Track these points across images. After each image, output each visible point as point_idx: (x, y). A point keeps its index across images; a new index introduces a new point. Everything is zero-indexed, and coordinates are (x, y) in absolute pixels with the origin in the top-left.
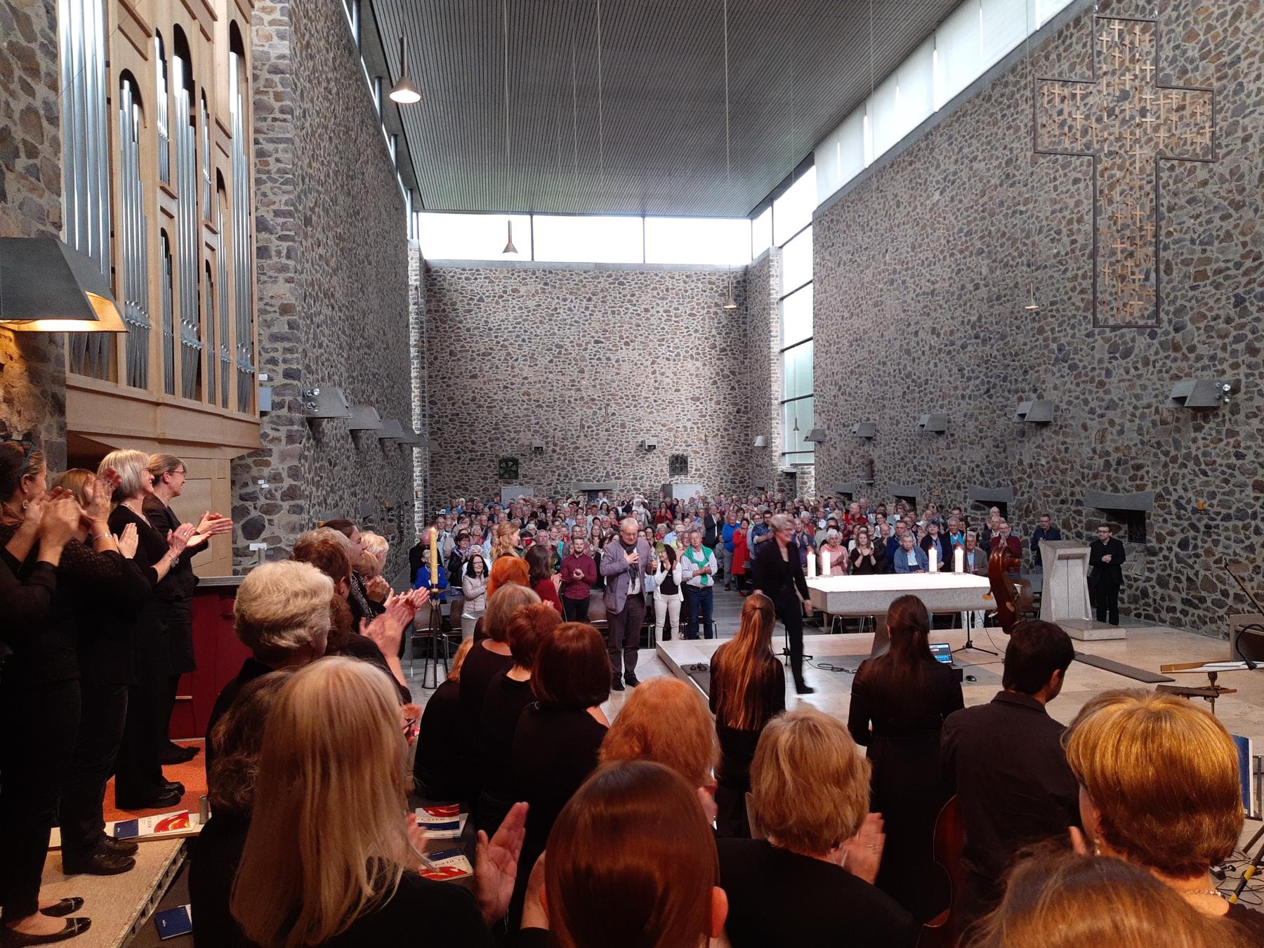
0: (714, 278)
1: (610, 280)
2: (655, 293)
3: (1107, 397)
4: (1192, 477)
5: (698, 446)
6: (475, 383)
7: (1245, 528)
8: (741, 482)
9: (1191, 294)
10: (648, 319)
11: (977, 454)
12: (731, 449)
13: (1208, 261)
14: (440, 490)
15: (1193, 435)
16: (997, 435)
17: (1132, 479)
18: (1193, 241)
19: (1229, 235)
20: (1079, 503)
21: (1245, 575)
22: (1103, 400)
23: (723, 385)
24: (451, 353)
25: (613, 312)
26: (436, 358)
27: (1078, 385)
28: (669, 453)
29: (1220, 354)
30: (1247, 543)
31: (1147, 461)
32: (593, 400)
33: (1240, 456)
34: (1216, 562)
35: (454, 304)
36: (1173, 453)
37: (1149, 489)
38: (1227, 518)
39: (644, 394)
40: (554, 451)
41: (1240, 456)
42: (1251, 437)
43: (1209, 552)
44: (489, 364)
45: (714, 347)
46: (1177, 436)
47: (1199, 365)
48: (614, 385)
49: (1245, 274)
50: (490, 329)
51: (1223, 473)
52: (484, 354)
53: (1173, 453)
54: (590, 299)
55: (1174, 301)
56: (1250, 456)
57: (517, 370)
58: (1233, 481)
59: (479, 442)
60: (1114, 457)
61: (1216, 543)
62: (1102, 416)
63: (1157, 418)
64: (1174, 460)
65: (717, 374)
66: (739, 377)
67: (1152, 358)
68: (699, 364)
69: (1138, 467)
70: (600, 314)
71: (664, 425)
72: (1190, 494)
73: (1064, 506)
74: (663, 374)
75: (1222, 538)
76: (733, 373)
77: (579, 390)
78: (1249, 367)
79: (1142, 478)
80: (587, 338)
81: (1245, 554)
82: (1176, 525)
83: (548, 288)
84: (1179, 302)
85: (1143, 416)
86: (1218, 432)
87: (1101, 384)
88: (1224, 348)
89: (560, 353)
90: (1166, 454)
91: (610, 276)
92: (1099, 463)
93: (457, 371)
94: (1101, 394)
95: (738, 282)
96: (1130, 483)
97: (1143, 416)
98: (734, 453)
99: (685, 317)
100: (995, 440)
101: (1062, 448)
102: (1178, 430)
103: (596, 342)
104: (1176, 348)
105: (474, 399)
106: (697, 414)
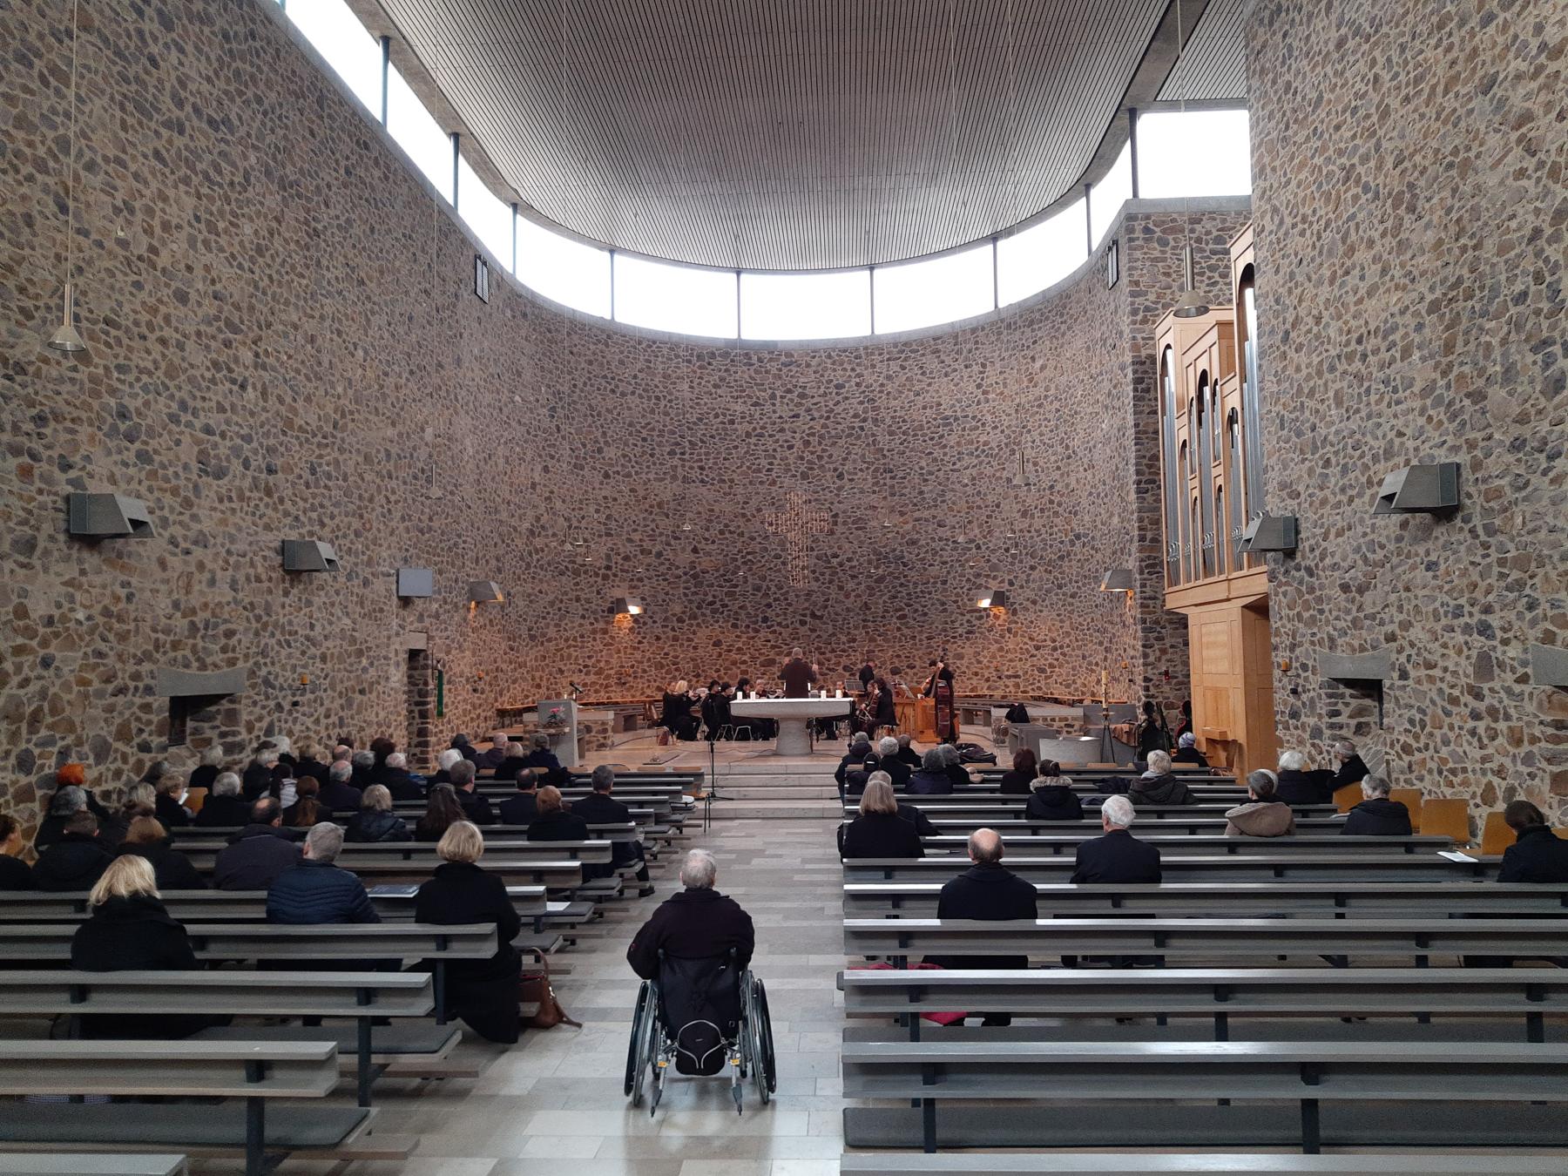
3: (195, 526)
4: (277, 648)
17: (224, 650)
20: (149, 690)
31: (239, 626)
36: (265, 618)
37: (240, 664)
46: (269, 598)
53: (265, 618)
58: (309, 653)
61: (295, 720)
62: (188, 553)
67: (248, 494)
69: (229, 634)
73: (121, 699)
79: (234, 650)
82: (264, 707)
85: (237, 566)
87: (187, 503)
90: (258, 618)
92: (180, 624)
94: (186, 518)
96: (222, 656)
101: (122, 592)
102: (270, 591)
104: (269, 493)
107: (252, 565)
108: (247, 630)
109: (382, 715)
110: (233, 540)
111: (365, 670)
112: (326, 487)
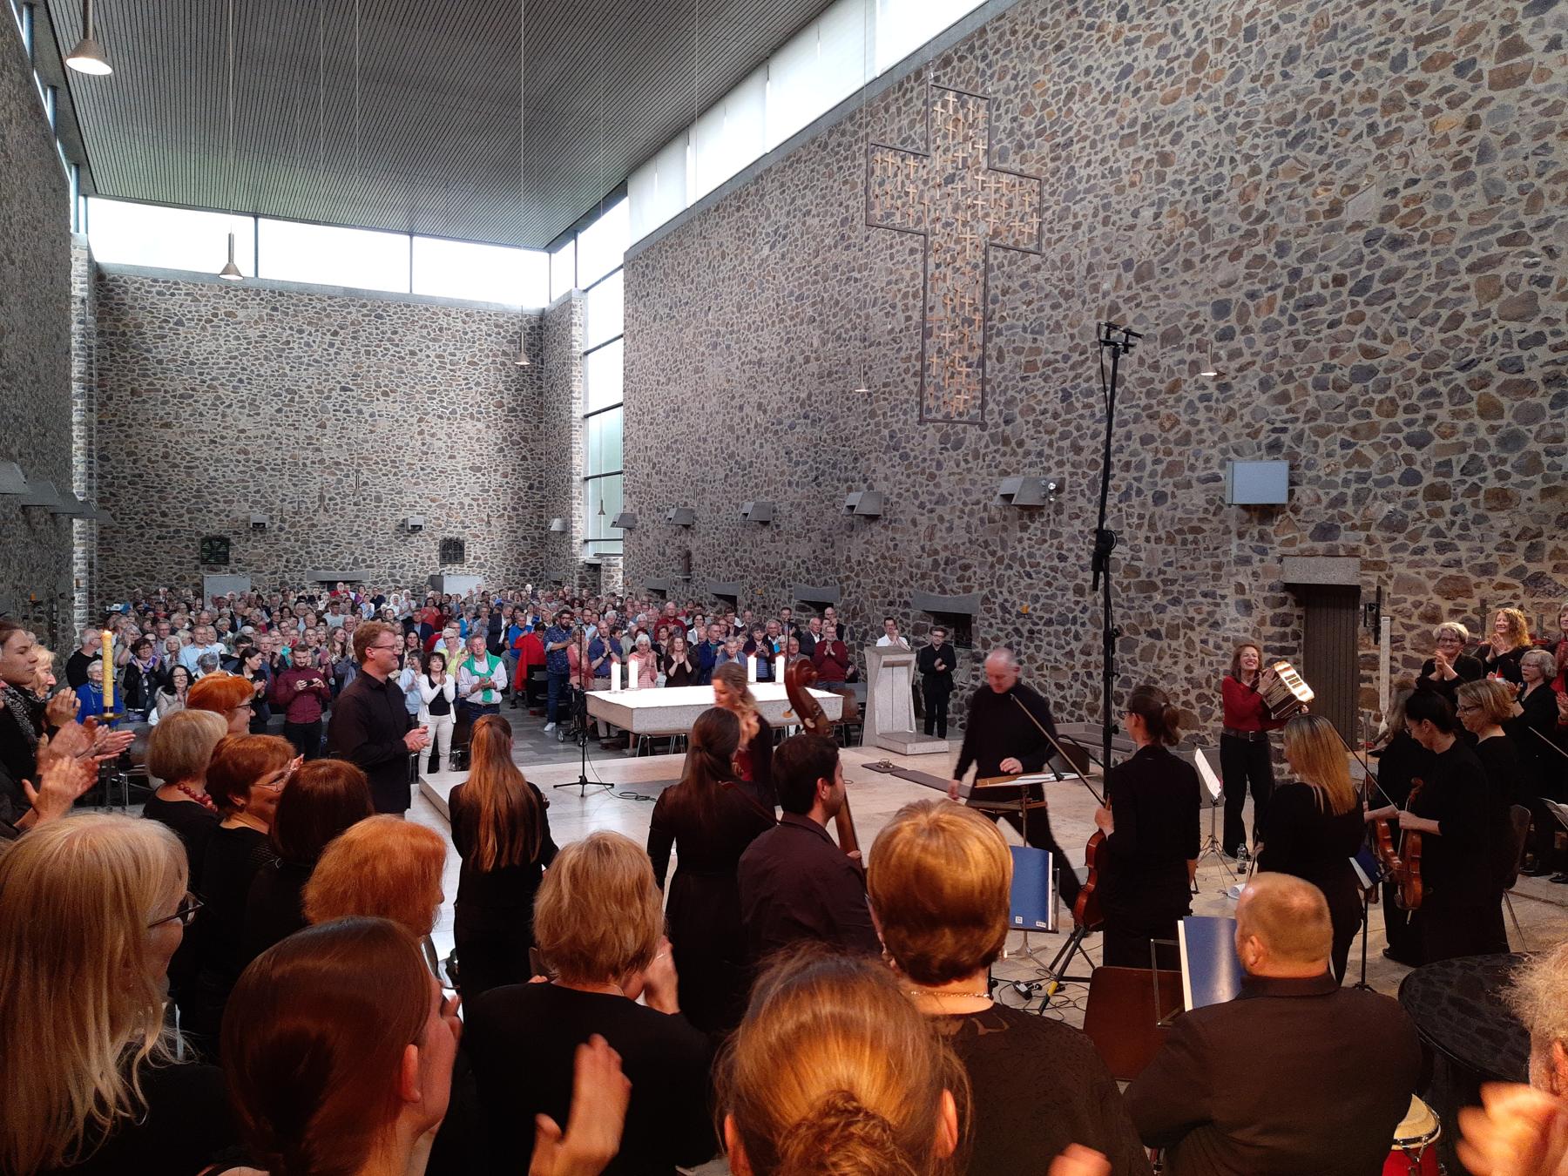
0: (501, 320)
1: (365, 311)
2: (425, 332)
3: (937, 491)
5: (479, 527)
6: (168, 434)
7: (1066, 633)
8: (532, 574)
9: (1021, 385)
10: (414, 364)
11: (803, 549)
12: (520, 533)
13: (1038, 351)
14: (112, 577)
15: (1019, 534)
16: (825, 527)
17: (960, 580)
18: (1025, 329)
19: (1058, 325)
20: (907, 604)
21: (1064, 682)
22: (933, 494)
23: (513, 456)
24: (133, 392)
25: (367, 353)
26: (110, 398)
27: (908, 476)
28: (439, 536)
29: (1047, 451)
30: (1068, 649)
31: (974, 561)
32: (338, 464)
33: (1062, 558)
34: (1037, 669)
35: (140, 326)
36: (1000, 553)
37: (975, 591)
38: (1049, 622)
39: (407, 459)
40: (281, 529)
41: (1062, 558)
42: (1073, 538)
43: (1031, 659)
44: (189, 410)
45: (500, 405)
47: (1027, 461)
48: (366, 446)
49: (1072, 368)
50: (192, 363)
51: (1047, 575)
52: (182, 396)
53: (1000, 553)
54: (335, 333)
55: (1005, 392)
56: (1072, 559)
57: (230, 420)
58: (1055, 584)
59: (172, 513)
60: (943, 555)
62: (932, 511)
63: (985, 515)
64: (1000, 560)
65: (505, 439)
66: (532, 445)
67: (983, 451)
68: (480, 425)
69: (966, 567)
70: (349, 355)
71: (433, 501)
72: (1015, 598)
73: (892, 608)
74: (433, 435)
75: (1044, 644)
76: (525, 439)
77: (318, 450)
78: (1073, 465)
79: (969, 579)
80: (331, 383)
81: (1064, 661)
82: (1001, 630)
83: (278, 315)
84: (1010, 393)
85: (971, 514)
86: (1043, 532)
87: (932, 476)
88: (1050, 445)
89: (292, 400)
90: (993, 553)
91: (364, 306)
92: (927, 562)
93: (141, 417)
94: (931, 488)
95: (532, 328)
97: (971, 514)
98: (524, 538)
99: (463, 365)
100: (823, 533)
101: (891, 544)
102: (1005, 529)
103: (344, 389)
104: (1006, 442)
105: (166, 455)
106: (477, 489)
107: (985, 508)
108: (981, 564)
109: (1198, 672)
110: (967, 492)
111: (1160, 609)
112: (1085, 406)
